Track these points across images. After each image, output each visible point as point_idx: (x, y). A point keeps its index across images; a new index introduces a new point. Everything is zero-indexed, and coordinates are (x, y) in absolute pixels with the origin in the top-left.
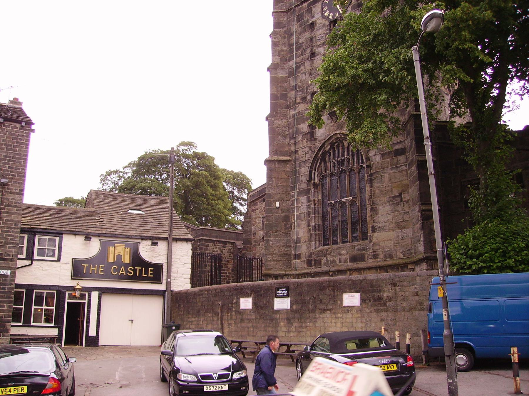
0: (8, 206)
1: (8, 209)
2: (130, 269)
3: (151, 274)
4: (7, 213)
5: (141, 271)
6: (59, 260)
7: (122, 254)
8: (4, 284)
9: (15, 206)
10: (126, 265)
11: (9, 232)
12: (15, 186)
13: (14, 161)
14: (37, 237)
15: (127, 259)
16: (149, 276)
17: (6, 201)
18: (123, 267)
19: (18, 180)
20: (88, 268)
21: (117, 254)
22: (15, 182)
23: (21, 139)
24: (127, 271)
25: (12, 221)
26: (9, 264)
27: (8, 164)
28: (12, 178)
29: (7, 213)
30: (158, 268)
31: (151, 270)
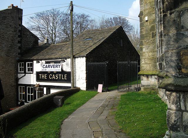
2: (57, 76)
6: (33, 73)
14: (27, 63)
20: (41, 76)
24: (55, 77)
30: (69, 74)
31: (66, 76)
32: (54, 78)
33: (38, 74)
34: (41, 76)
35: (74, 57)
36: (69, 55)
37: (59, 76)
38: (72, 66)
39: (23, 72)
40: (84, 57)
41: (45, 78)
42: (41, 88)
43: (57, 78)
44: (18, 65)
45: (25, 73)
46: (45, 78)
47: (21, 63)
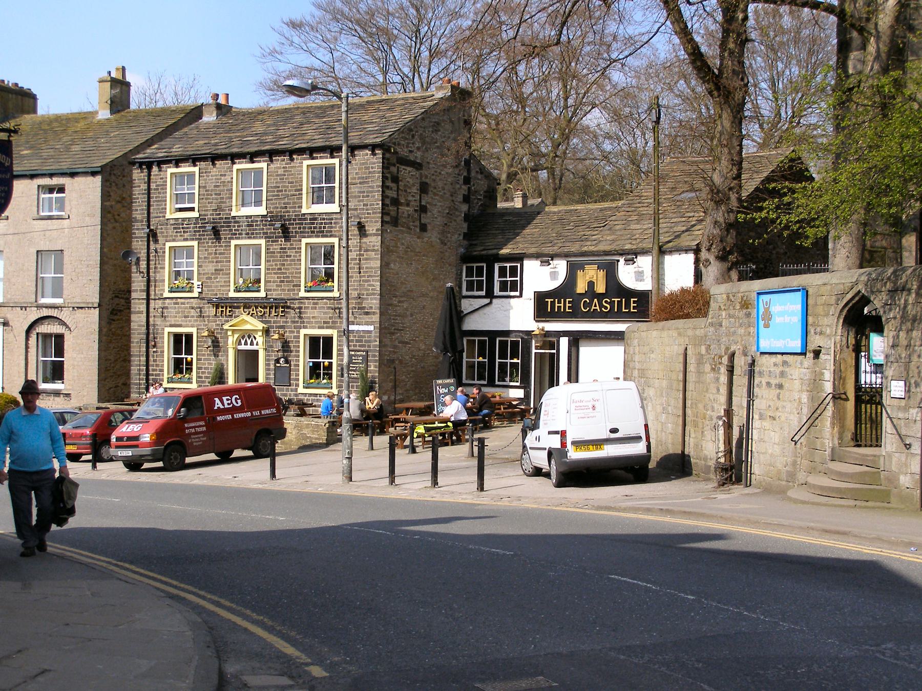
0: (367, 251)
1: (367, 255)
2: (606, 302)
3: (634, 308)
4: (366, 259)
5: (620, 303)
6: (521, 296)
7: (594, 280)
8: (369, 341)
9: (374, 250)
10: (600, 297)
11: (369, 281)
12: (371, 226)
13: (368, 196)
14: (496, 267)
15: (601, 288)
16: (632, 310)
17: (364, 245)
18: (596, 300)
19: (374, 218)
20: (553, 303)
21: (588, 279)
22: (371, 222)
23: (372, 168)
24: (601, 306)
25: (371, 268)
26: (372, 318)
27: (363, 201)
28: (368, 217)
29: (366, 259)
31: (634, 302)
32: (598, 308)
33: (541, 299)
34: (553, 303)
35: (662, 252)
36: (647, 245)
37: (612, 304)
38: (655, 275)
39: (483, 293)
40: (691, 250)
41: (567, 310)
42: (550, 340)
43: (606, 308)
44: (461, 273)
45: (490, 295)
46: (567, 310)
47: (475, 265)
